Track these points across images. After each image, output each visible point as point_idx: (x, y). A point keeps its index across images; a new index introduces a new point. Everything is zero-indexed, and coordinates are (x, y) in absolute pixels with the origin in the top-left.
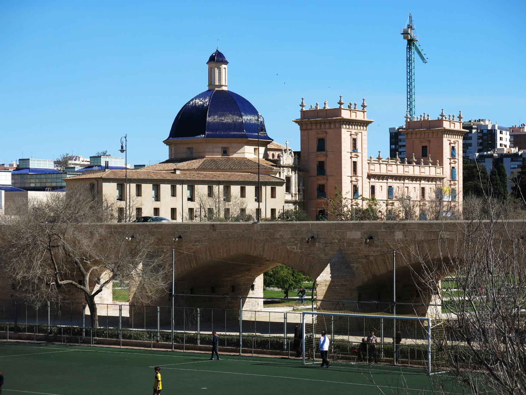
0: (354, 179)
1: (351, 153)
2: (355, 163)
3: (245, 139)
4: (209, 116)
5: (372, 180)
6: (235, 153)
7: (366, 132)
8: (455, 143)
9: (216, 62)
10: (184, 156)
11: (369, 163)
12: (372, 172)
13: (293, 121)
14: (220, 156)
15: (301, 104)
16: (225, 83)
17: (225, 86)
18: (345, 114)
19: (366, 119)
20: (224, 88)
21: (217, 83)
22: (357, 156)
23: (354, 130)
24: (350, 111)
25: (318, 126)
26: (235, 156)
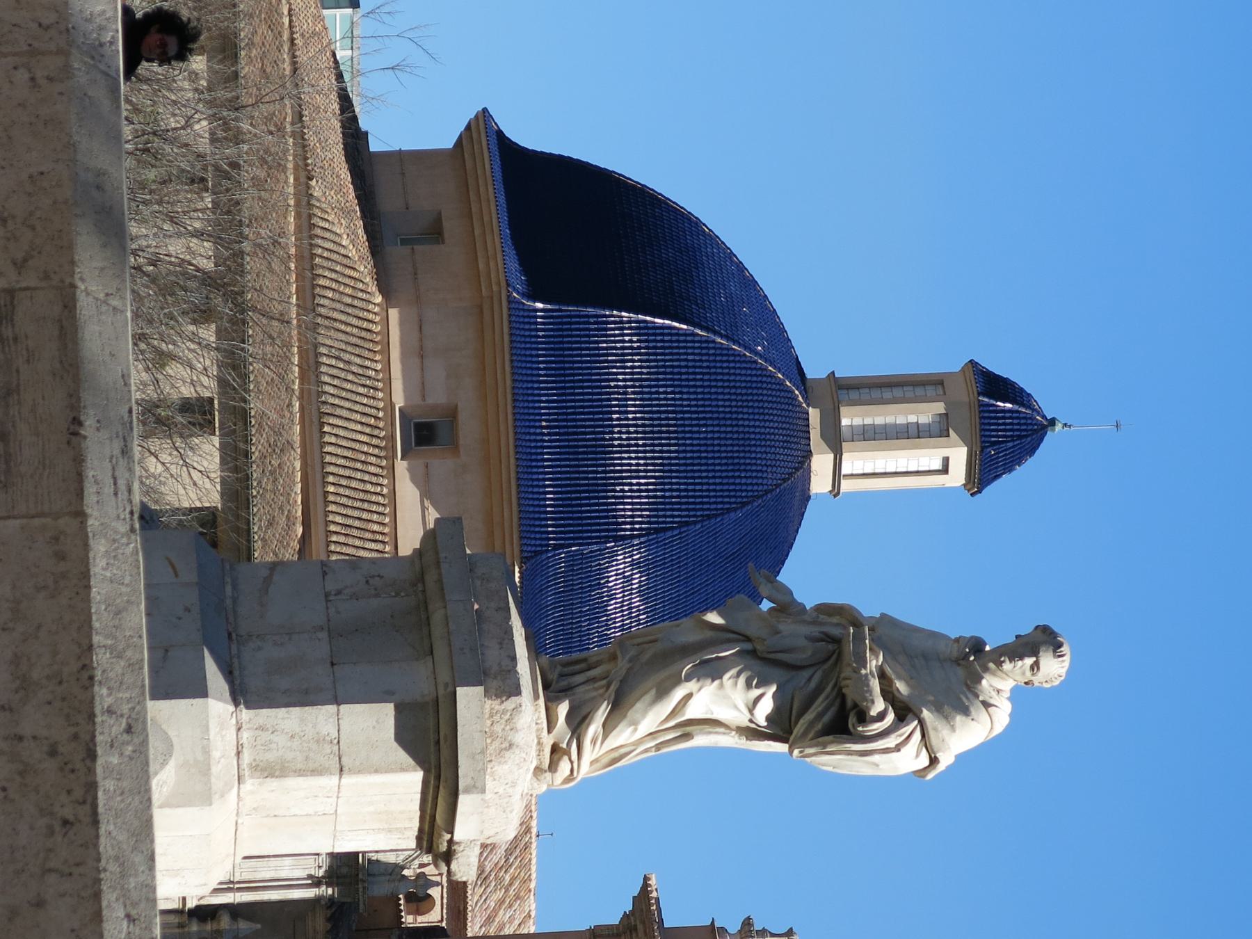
9: (981, 404)
10: (389, 201)
13: (646, 879)
14: (399, 401)
15: (757, 927)
16: (852, 476)
20: (821, 464)
21: (850, 418)
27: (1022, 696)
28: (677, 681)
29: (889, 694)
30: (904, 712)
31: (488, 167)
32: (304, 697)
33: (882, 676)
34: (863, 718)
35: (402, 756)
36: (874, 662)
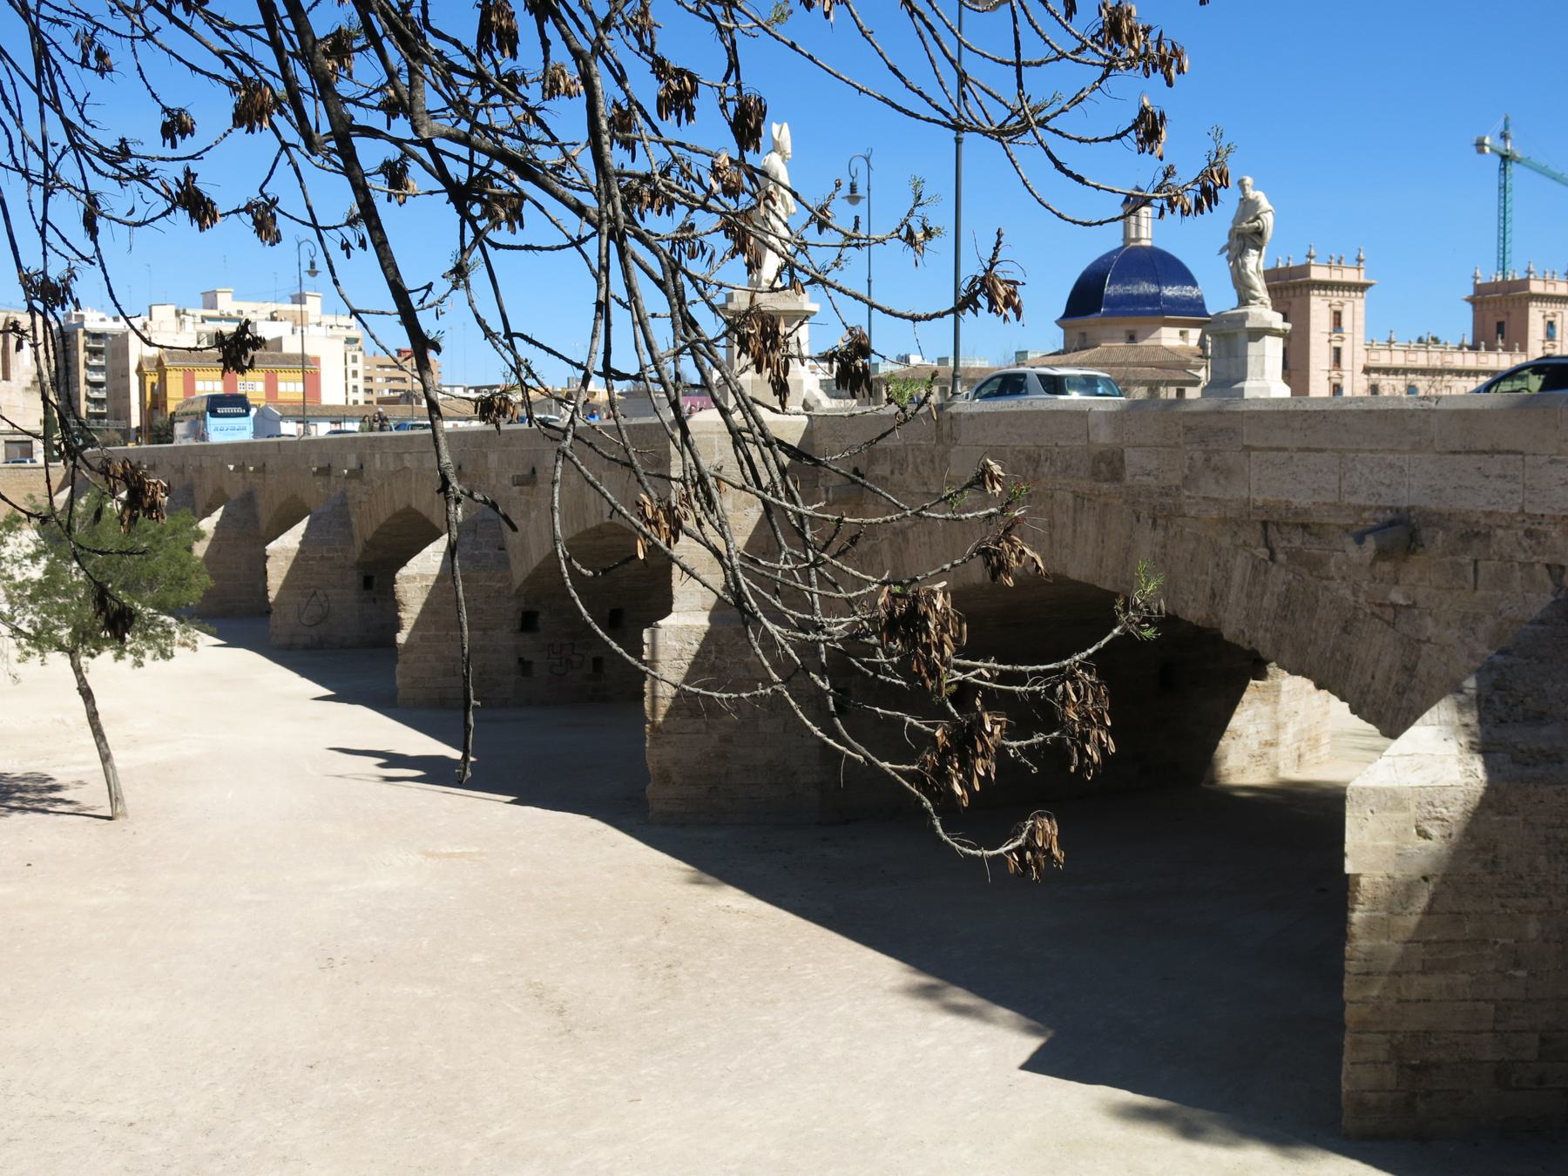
0: (1334, 374)
1: (1330, 334)
2: (1338, 351)
3: (1159, 318)
4: (1109, 285)
5: (1374, 376)
6: (1146, 338)
7: (1362, 302)
8: (1554, 315)
11: (1367, 350)
12: (1372, 364)
14: (1124, 344)
17: (1147, 239)
18: (1318, 274)
19: (1362, 280)
20: (1145, 243)
21: (1133, 235)
22: (1342, 339)
23: (1336, 297)
24: (1330, 267)
25: (1279, 294)
26: (1146, 342)
27: (1254, 189)
28: (1246, 274)
29: (1253, 221)
30: (1258, 218)
31: (1068, 321)
32: (1245, 364)
33: (1248, 223)
34: (1258, 228)
35: (1261, 340)
36: (1244, 225)
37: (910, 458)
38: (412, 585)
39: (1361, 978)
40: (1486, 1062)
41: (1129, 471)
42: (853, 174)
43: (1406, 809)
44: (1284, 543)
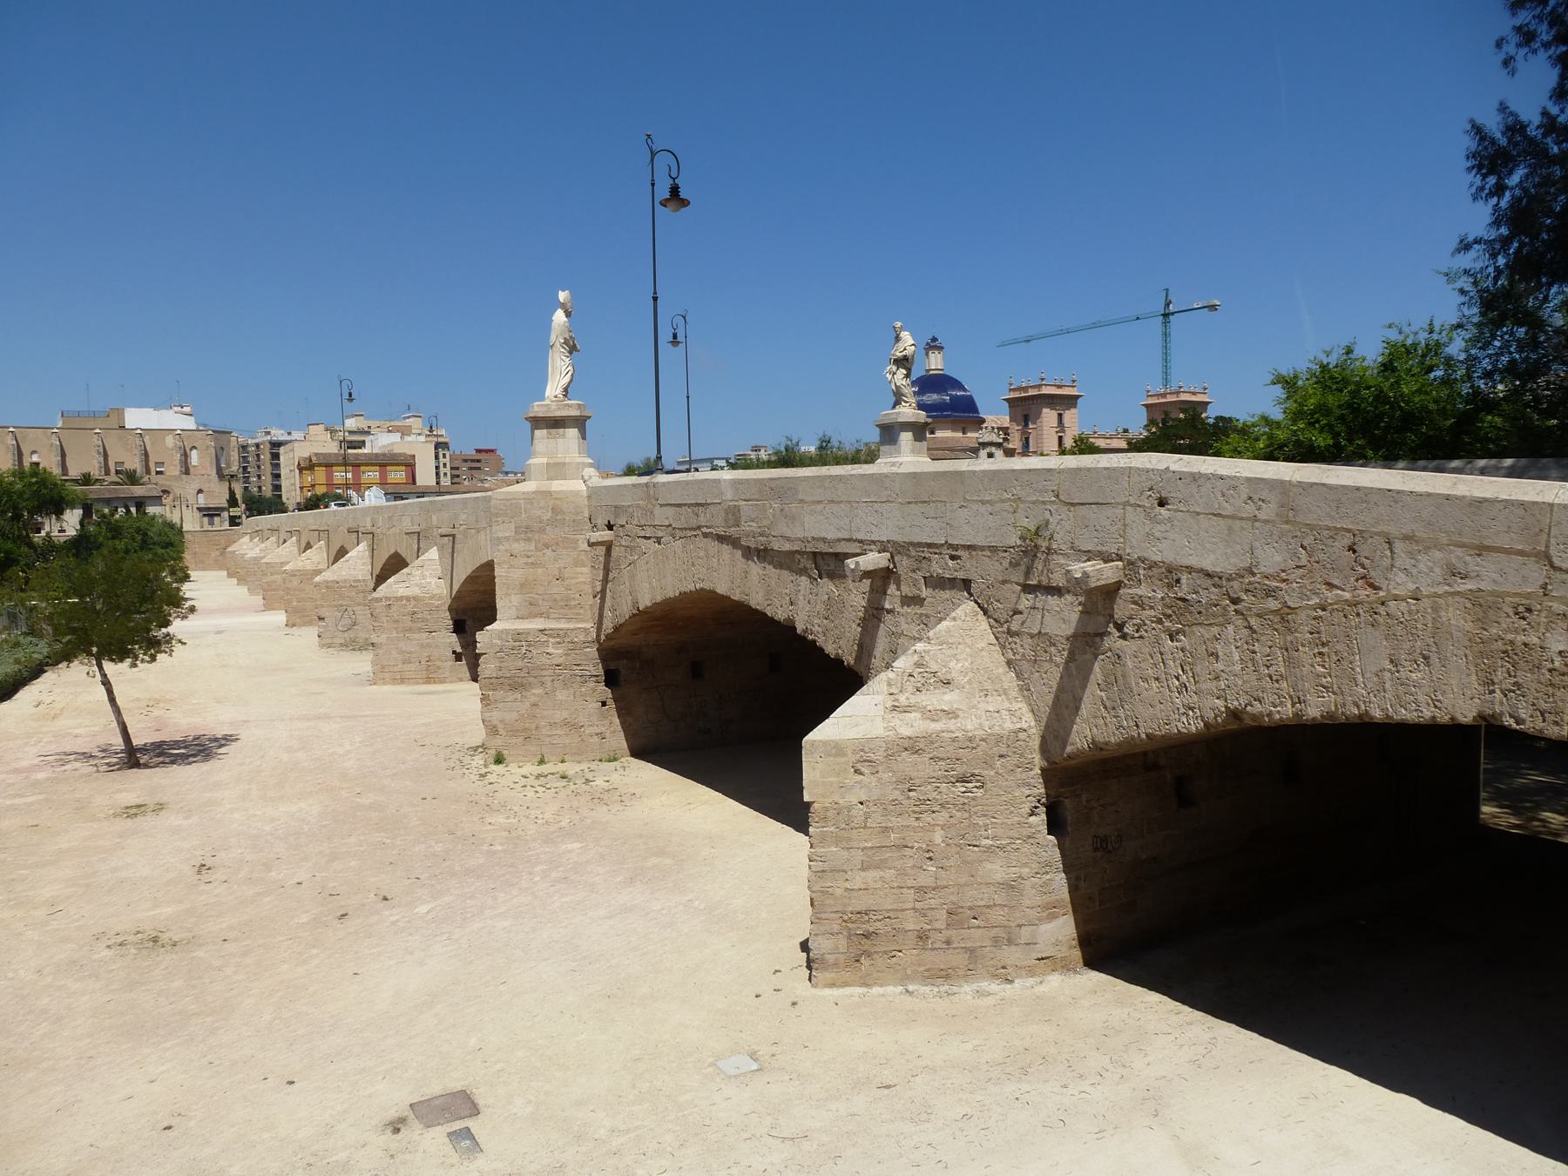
37: (635, 514)
38: (380, 604)
39: (819, 874)
40: (910, 931)
41: (743, 519)
42: (675, 327)
43: (845, 755)
44: (826, 567)
